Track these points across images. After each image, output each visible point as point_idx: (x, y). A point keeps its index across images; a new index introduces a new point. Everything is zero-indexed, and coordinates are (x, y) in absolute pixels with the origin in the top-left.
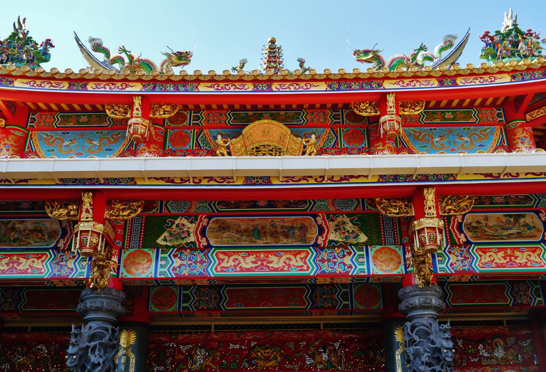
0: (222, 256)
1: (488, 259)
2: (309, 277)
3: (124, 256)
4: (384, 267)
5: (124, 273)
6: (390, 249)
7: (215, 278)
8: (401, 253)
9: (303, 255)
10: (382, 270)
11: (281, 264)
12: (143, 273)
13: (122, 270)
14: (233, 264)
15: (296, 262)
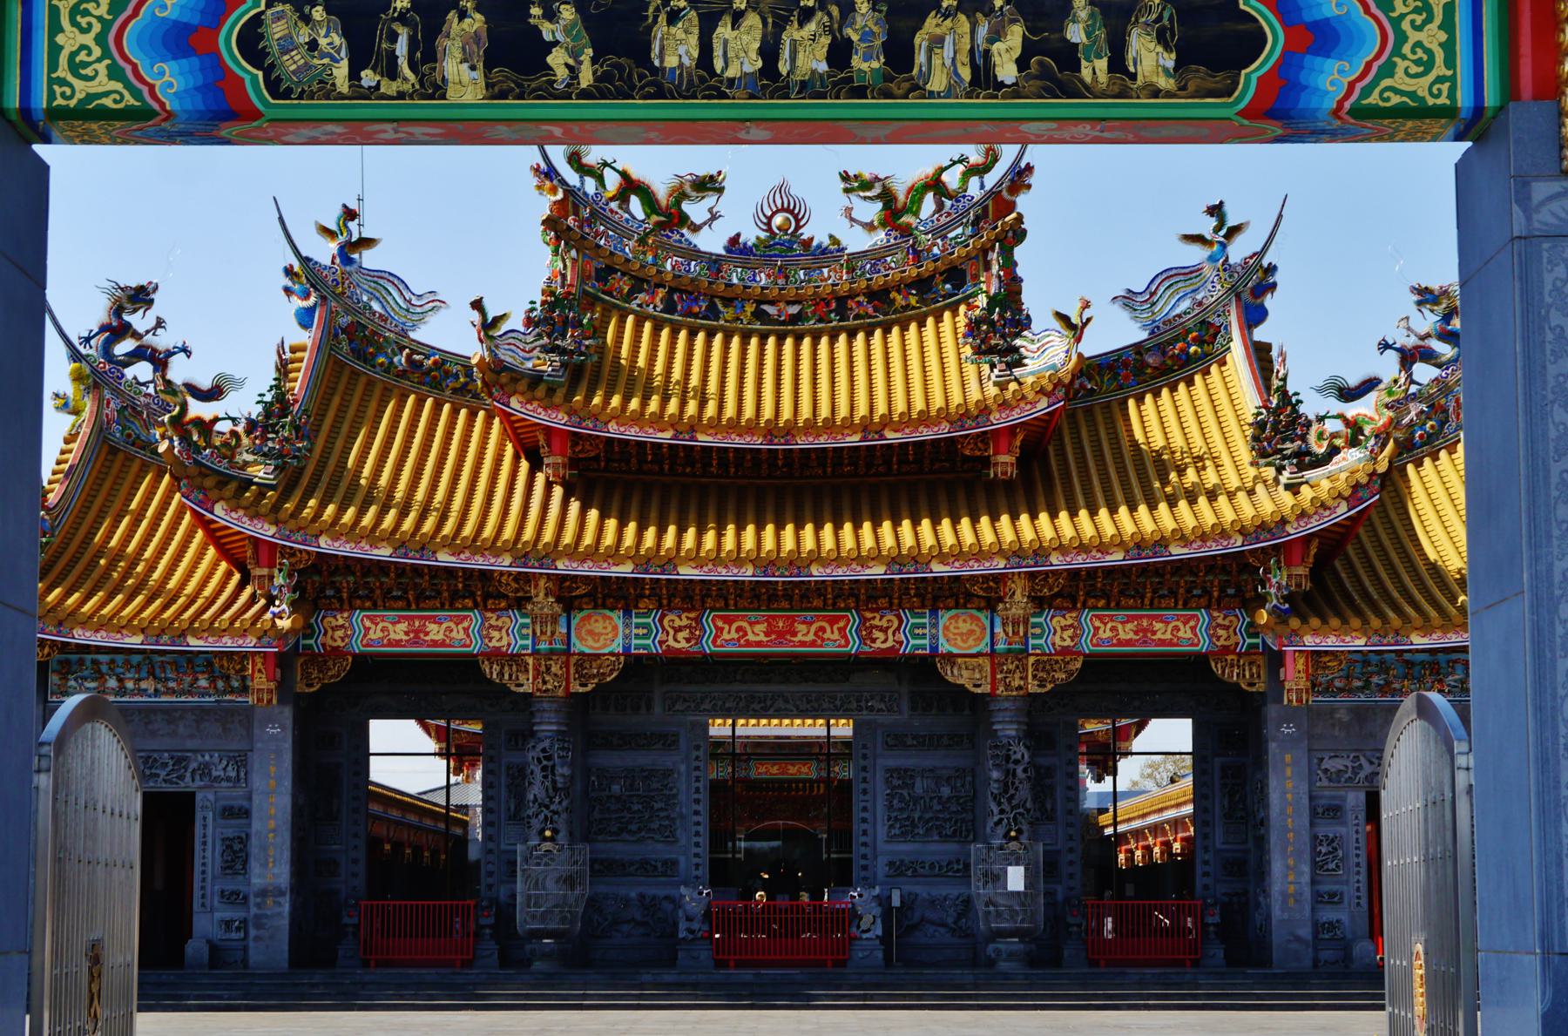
0: (720, 624)
1: (1108, 634)
2: (850, 655)
3: (574, 623)
4: (959, 642)
5: (578, 646)
6: (972, 616)
7: (712, 655)
8: (987, 623)
9: (841, 624)
10: (955, 645)
11: (811, 637)
12: (605, 646)
13: (574, 639)
14: (736, 636)
15: (832, 634)
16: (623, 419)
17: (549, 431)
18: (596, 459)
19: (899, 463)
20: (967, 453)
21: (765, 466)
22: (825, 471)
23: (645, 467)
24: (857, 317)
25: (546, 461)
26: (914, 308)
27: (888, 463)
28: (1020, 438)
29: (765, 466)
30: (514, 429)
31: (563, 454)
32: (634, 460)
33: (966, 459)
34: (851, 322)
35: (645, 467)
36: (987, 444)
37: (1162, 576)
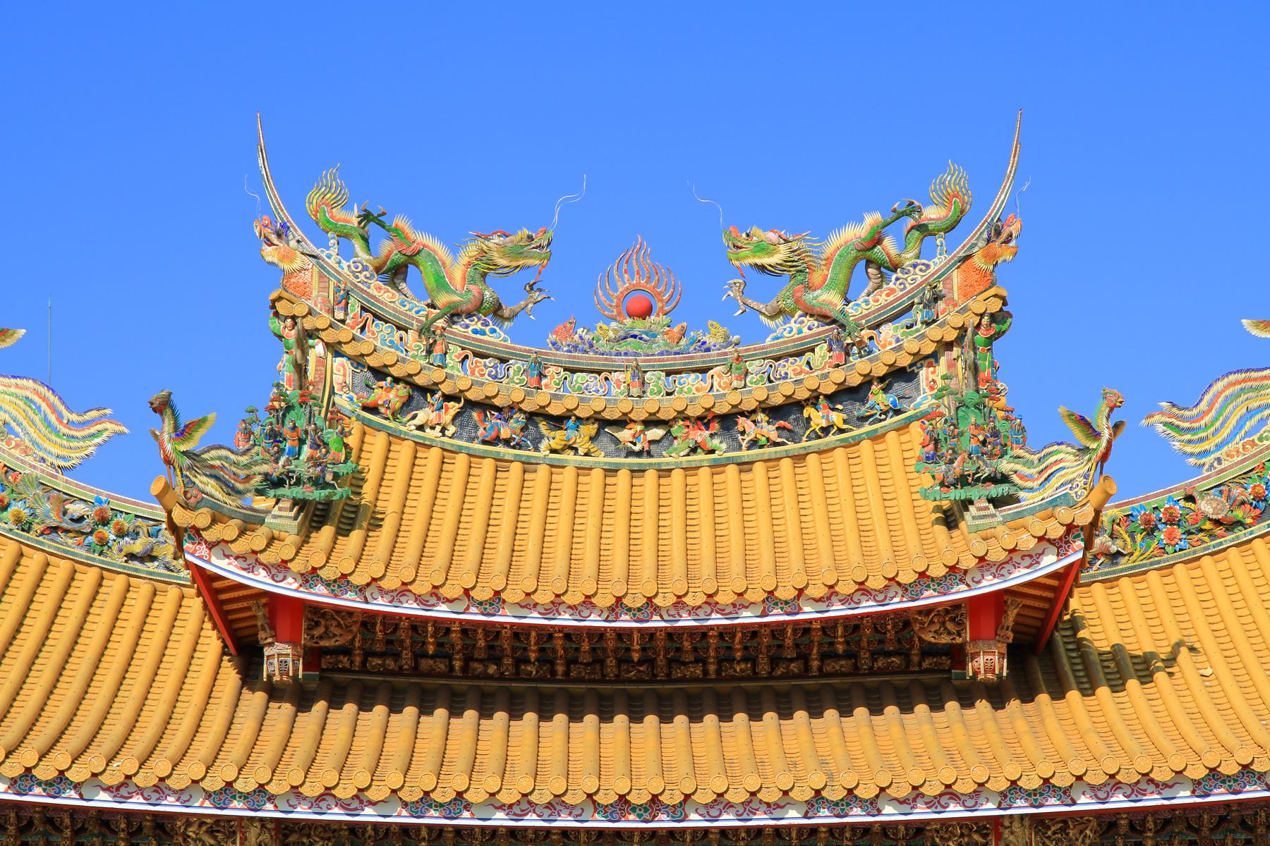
16: (380, 573)
17: (275, 602)
18: (346, 651)
19: (823, 657)
20: (929, 637)
21: (611, 662)
22: (705, 672)
23: (425, 664)
24: (754, 444)
25: (267, 651)
26: (841, 431)
27: (804, 658)
28: (1012, 614)
29: (611, 662)
30: (219, 604)
31: (293, 642)
32: (406, 655)
33: (930, 650)
34: (745, 454)
35: (425, 664)
36: (960, 624)
37: (1251, 830)
